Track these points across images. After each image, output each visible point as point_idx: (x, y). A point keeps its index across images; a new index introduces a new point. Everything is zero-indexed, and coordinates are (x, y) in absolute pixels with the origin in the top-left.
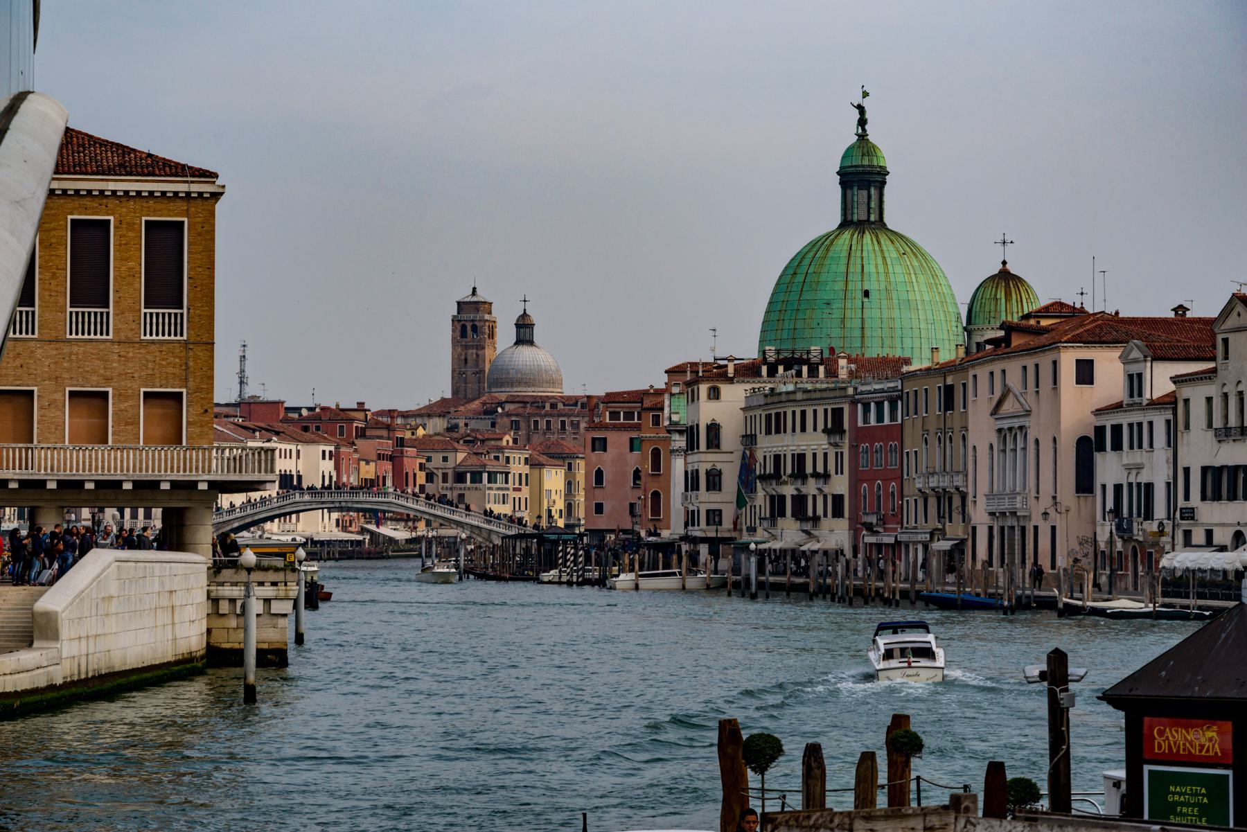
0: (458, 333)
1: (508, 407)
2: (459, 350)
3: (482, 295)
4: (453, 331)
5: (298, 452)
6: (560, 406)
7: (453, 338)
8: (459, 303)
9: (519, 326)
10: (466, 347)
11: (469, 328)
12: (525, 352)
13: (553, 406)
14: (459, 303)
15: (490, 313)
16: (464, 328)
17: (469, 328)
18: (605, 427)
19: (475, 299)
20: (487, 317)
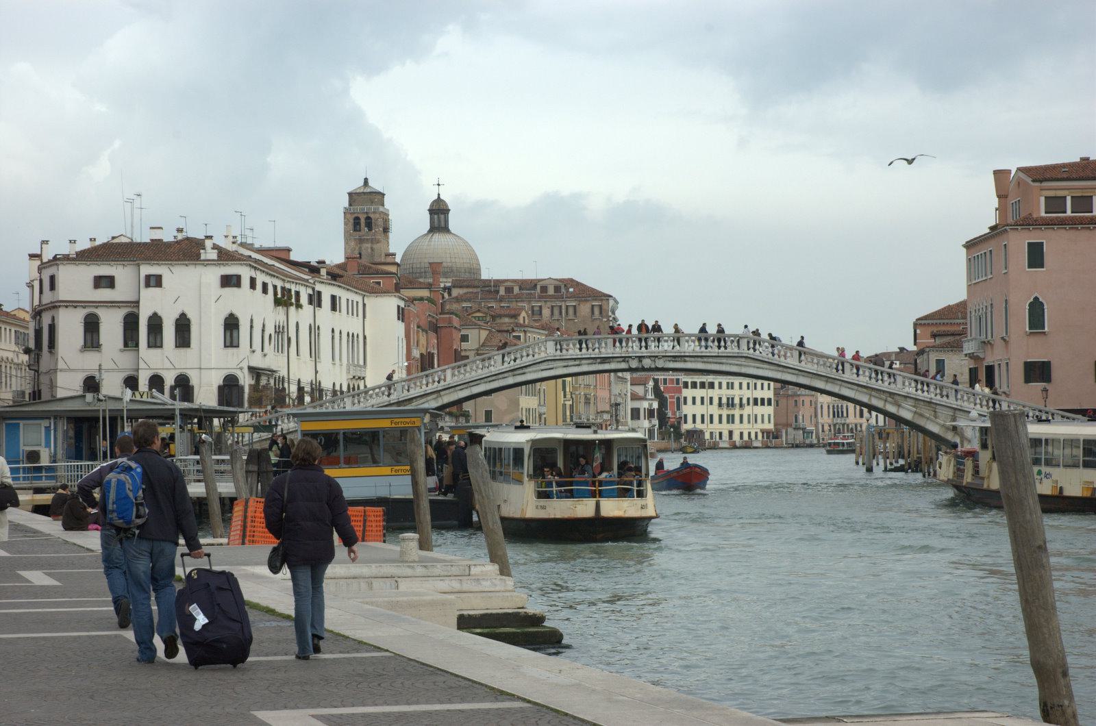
0: (351, 226)
1: (455, 292)
2: (353, 244)
3: (375, 185)
4: (346, 224)
5: (364, 305)
6: (516, 290)
7: (346, 232)
8: (350, 194)
9: (432, 211)
10: (361, 241)
11: (363, 221)
12: (439, 238)
13: (509, 290)
14: (350, 194)
15: (383, 205)
16: (357, 221)
17: (363, 221)
18: (1048, 223)
19: (368, 190)
20: (381, 209)
